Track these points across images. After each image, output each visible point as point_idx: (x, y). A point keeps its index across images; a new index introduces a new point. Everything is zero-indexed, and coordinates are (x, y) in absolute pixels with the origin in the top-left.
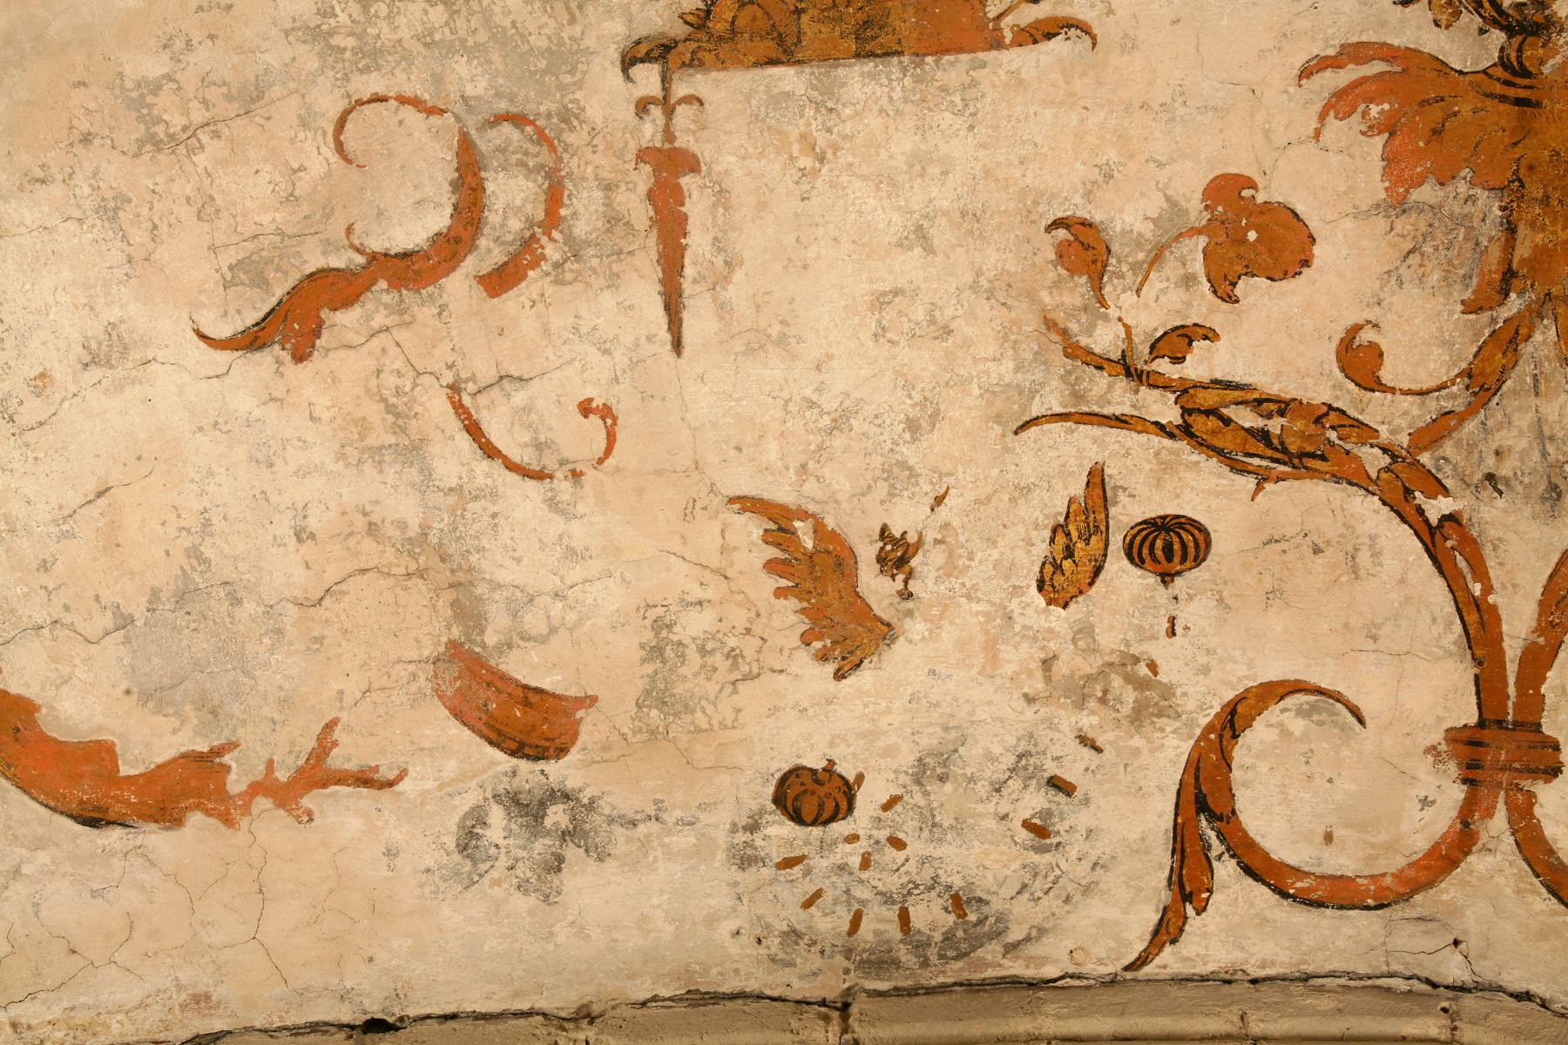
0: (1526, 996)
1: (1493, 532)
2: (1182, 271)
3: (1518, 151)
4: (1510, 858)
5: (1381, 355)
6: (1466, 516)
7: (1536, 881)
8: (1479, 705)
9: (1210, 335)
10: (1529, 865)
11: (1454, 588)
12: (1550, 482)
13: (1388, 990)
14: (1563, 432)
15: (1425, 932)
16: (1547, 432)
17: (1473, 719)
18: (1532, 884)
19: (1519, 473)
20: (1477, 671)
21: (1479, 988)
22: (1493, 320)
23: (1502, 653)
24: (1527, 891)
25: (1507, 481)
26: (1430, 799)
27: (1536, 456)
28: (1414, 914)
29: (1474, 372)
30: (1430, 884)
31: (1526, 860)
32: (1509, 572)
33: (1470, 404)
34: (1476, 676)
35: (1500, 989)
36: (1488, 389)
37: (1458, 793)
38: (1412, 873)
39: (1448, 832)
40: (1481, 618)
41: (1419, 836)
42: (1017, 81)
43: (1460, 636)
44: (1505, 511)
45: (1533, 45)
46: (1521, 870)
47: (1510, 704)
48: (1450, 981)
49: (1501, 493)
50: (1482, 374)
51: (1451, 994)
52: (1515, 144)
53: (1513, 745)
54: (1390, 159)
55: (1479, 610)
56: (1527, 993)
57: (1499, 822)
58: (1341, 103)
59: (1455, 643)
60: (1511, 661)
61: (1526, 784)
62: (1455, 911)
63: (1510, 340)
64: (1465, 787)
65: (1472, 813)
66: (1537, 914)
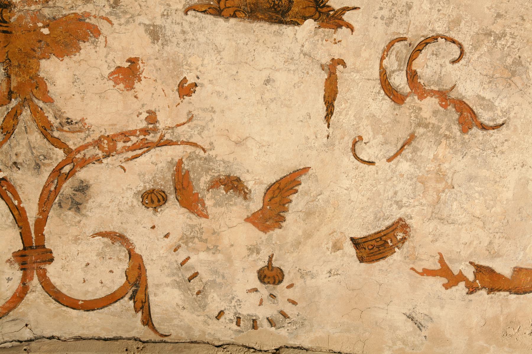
0: (53, 337)
1: (19, 182)
3: (7, 49)
4: (41, 292)
6: (8, 178)
7: (51, 298)
8: (23, 242)
10: (48, 293)
11: (8, 203)
12: (36, 163)
13: (5, 348)
14: (38, 145)
15: (15, 324)
16: (32, 146)
17: (21, 247)
18: (49, 299)
19: (25, 161)
20: (20, 231)
21: (36, 339)
22: (8, 109)
23: (28, 223)
24: (48, 302)
25: (21, 164)
26: (10, 278)
27: (30, 154)
28: (11, 319)
29: (4, 127)
30: (15, 307)
31: (46, 292)
32: (26, 195)
33: (4, 138)
34: (21, 233)
35: (44, 337)
36: (9, 133)
37: (20, 274)
38: (8, 305)
39: (18, 288)
40: (19, 212)
41: (8, 292)
43: (13, 220)
44: (22, 174)
45: (6, 12)
46: (45, 295)
47: (33, 240)
48: (26, 339)
49: (19, 169)
50: (6, 128)
51: (27, 343)
52: (5, 46)
53: (37, 254)
55: (18, 210)
56: (53, 336)
57: (35, 281)
59: (11, 222)
60: (32, 226)
61: (43, 266)
62: (25, 314)
63: (15, 115)
64: (22, 272)
65: (26, 280)
66: (52, 309)
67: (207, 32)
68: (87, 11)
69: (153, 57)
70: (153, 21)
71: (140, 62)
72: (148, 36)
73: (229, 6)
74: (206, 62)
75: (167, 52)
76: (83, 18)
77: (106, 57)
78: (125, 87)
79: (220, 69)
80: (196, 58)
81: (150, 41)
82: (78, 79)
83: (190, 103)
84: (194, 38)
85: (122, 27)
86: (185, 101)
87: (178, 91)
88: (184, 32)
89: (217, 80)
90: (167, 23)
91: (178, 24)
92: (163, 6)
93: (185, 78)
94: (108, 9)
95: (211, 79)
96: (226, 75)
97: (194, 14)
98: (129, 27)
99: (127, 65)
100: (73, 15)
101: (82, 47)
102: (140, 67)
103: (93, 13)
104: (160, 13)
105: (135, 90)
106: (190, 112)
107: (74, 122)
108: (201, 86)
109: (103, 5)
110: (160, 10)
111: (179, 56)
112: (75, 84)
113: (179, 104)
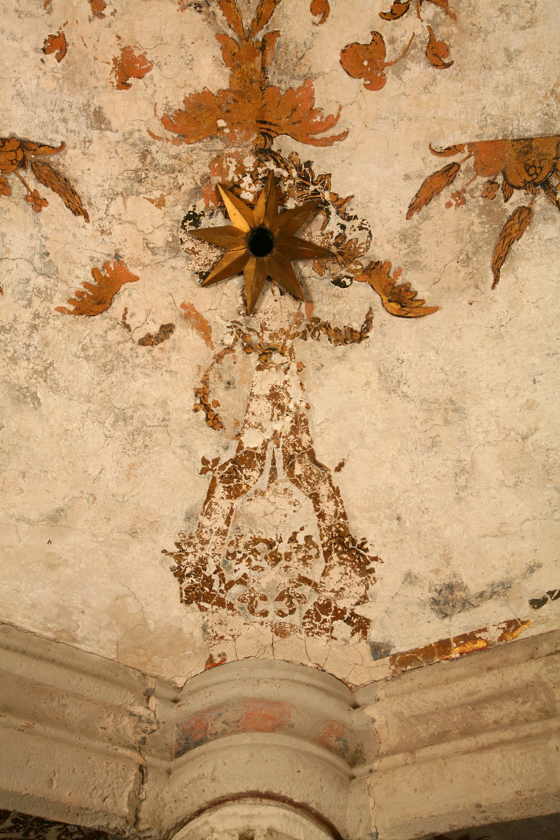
2: (395, 45)
3: (263, 102)
5: (311, 10)
9: (383, 15)
22: (267, 28)
29: (273, 4)
42: (463, 129)
45: (261, 145)
52: (264, 105)
54: (311, 98)
58: (332, 121)
67: (36, 120)
68: (175, 147)
69: (100, 89)
70: (101, 135)
71: (116, 84)
72: (106, 117)
73: (11, 153)
74: (34, 82)
75: (83, 96)
76: (181, 138)
77: (155, 91)
78: (132, 51)
79: (15, 71)
80: (47, 88)
81: (104, 110)
82: (187, 64)
83: (50, 26)
84: (51, 113)
85: (137, 128)
86: (57, 29)
87: (66, 44)
88: (64, 120)
89: (18, 57)
90: (85, 132)
91: (71, 131)
92: (91, 152)
93: (59, 61)
94: (153, 148)
95: (25, 59)
96: (6, 63)
97: (53, 143)
98: (129, 128)
99: (131, 81)
100: (191, 142)
101: (182, 103)
102: (116, 77)
103: (169, 143)
104: (94, 144)
105: (120, 47)
106: (49, 13)
107: (192, 7)
108: (37, 48)
109: (158, 154)
110: (94, 148)
111: (68, 90)
112: (191, 58)
113: (64, 25)
